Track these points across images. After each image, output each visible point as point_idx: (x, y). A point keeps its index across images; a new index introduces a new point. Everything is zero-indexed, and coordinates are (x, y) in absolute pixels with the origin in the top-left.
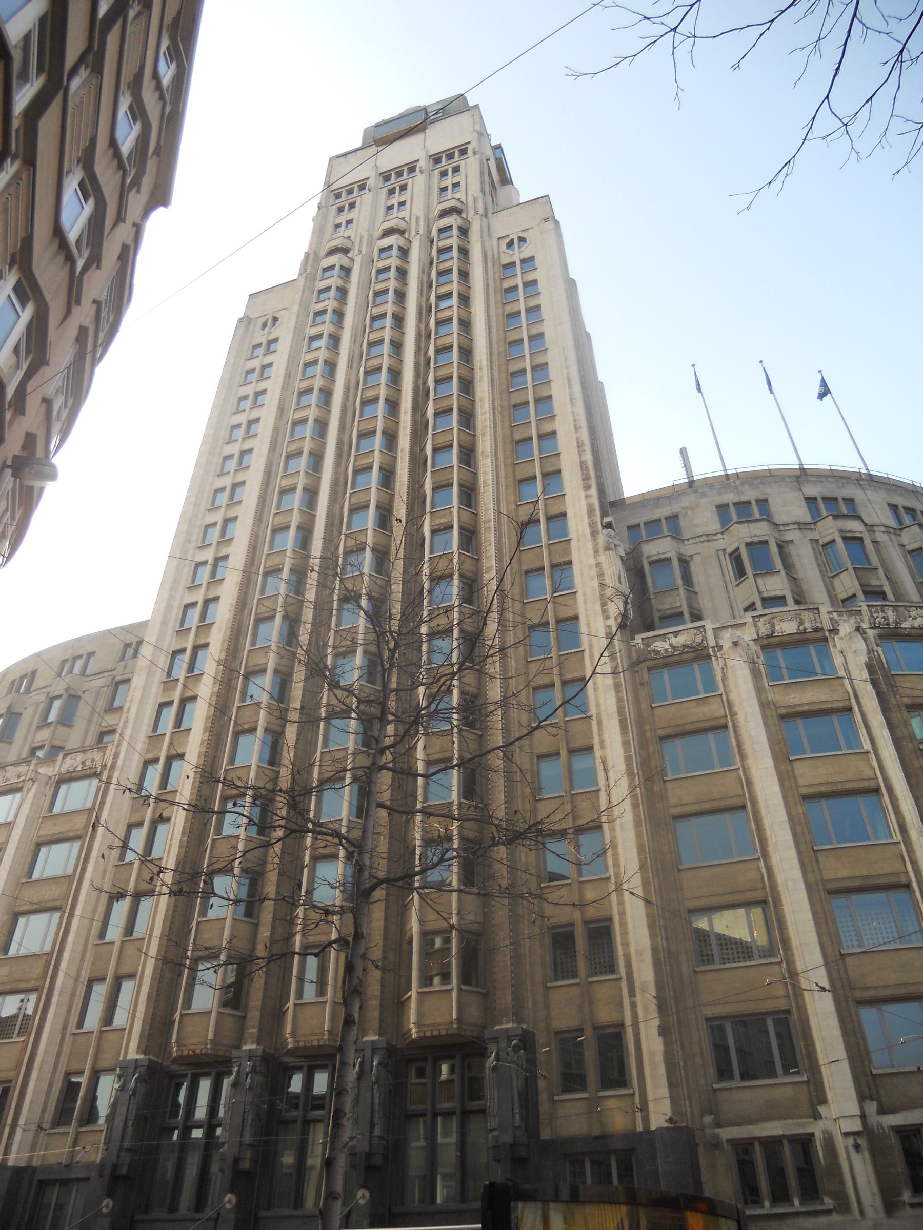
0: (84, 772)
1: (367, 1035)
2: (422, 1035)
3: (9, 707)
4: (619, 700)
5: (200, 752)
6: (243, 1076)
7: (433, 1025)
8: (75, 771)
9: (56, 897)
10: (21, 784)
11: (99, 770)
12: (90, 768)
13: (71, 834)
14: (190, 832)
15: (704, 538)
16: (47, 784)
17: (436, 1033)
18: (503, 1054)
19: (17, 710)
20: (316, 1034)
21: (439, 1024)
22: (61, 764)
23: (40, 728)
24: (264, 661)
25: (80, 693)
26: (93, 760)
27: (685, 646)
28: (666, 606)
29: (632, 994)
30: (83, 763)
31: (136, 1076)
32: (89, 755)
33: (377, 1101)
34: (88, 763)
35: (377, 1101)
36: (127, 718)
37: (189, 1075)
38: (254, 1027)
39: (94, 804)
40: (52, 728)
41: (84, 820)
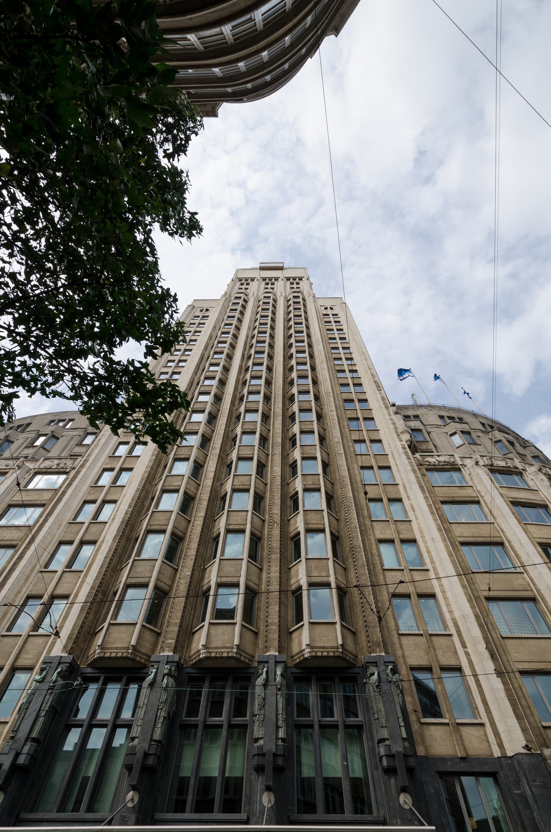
0: (57, 470)
1: (268, 651)
2: (314, 654)
3: (7, 436)
4: (417, 477)
5: (148, 465)
6: (159, 678)
7: (323, 647)
8: (50, 468)
9: (15, 538)
10: (7, 470)
11: (68, 470)
12: (62, 468)
13: (38, 502)
14: (134, 507)
15: (435, 426)
16: (28, 472)
17: (325, 654)
18: (383, 676)
19: (11, 439)
20: (227, 648)
21: (327, 648)
22: (41, 463)
23: (26, 447)
24: (197, 428)
25: (60, 437)
26: (65, 464)
27: (445, 462)
28: (424, 448)
29: (464, 646)
30: (58, 465)
31: (59, 670)
32: (64, 461)
33: (280, 706)
34: (62, 465)
35: (280, 706)
36: (98, 443)
37: (102, 678)
38: (172, 639)
39: (60, 487)
40: (37, 448)
41: (50, 495)
